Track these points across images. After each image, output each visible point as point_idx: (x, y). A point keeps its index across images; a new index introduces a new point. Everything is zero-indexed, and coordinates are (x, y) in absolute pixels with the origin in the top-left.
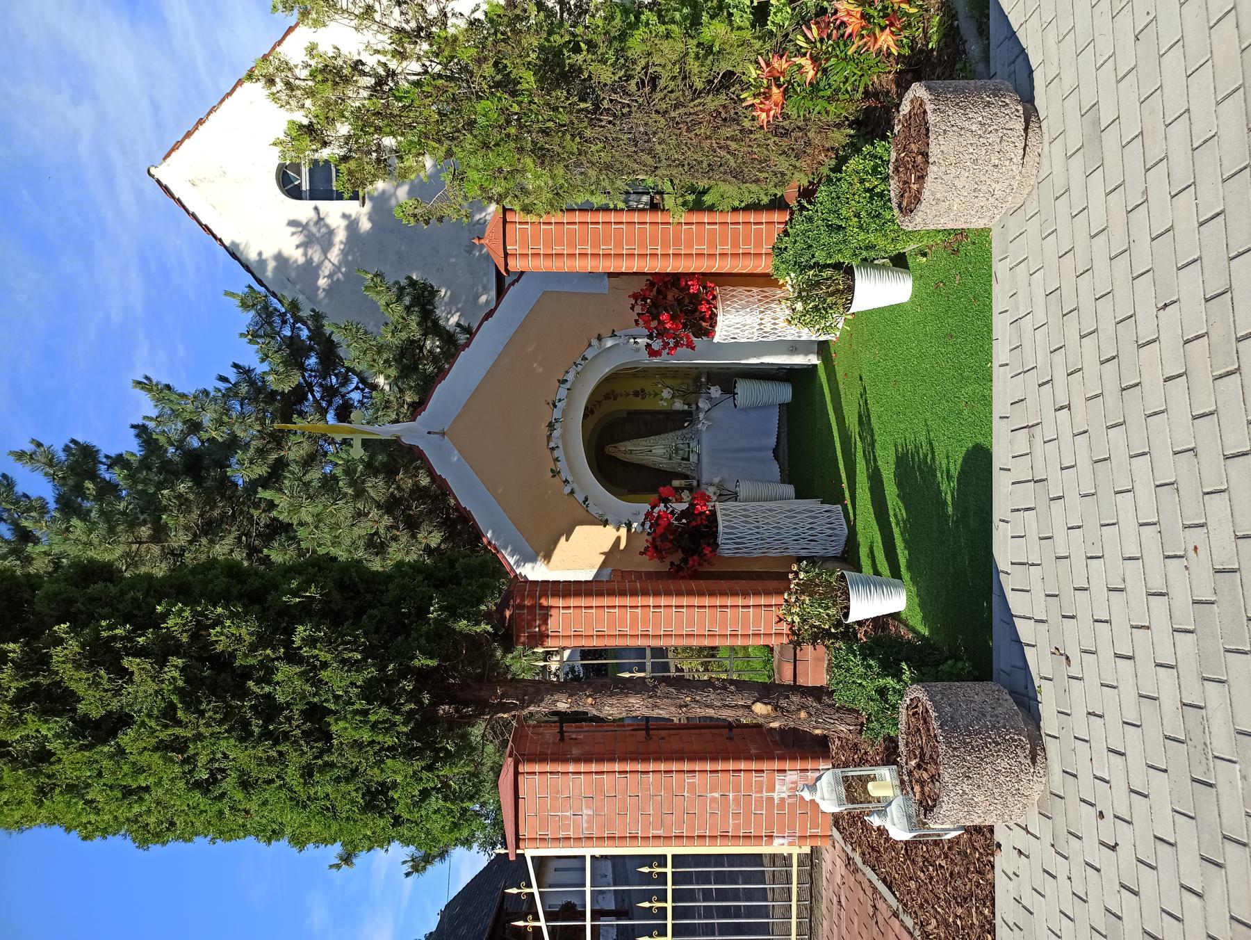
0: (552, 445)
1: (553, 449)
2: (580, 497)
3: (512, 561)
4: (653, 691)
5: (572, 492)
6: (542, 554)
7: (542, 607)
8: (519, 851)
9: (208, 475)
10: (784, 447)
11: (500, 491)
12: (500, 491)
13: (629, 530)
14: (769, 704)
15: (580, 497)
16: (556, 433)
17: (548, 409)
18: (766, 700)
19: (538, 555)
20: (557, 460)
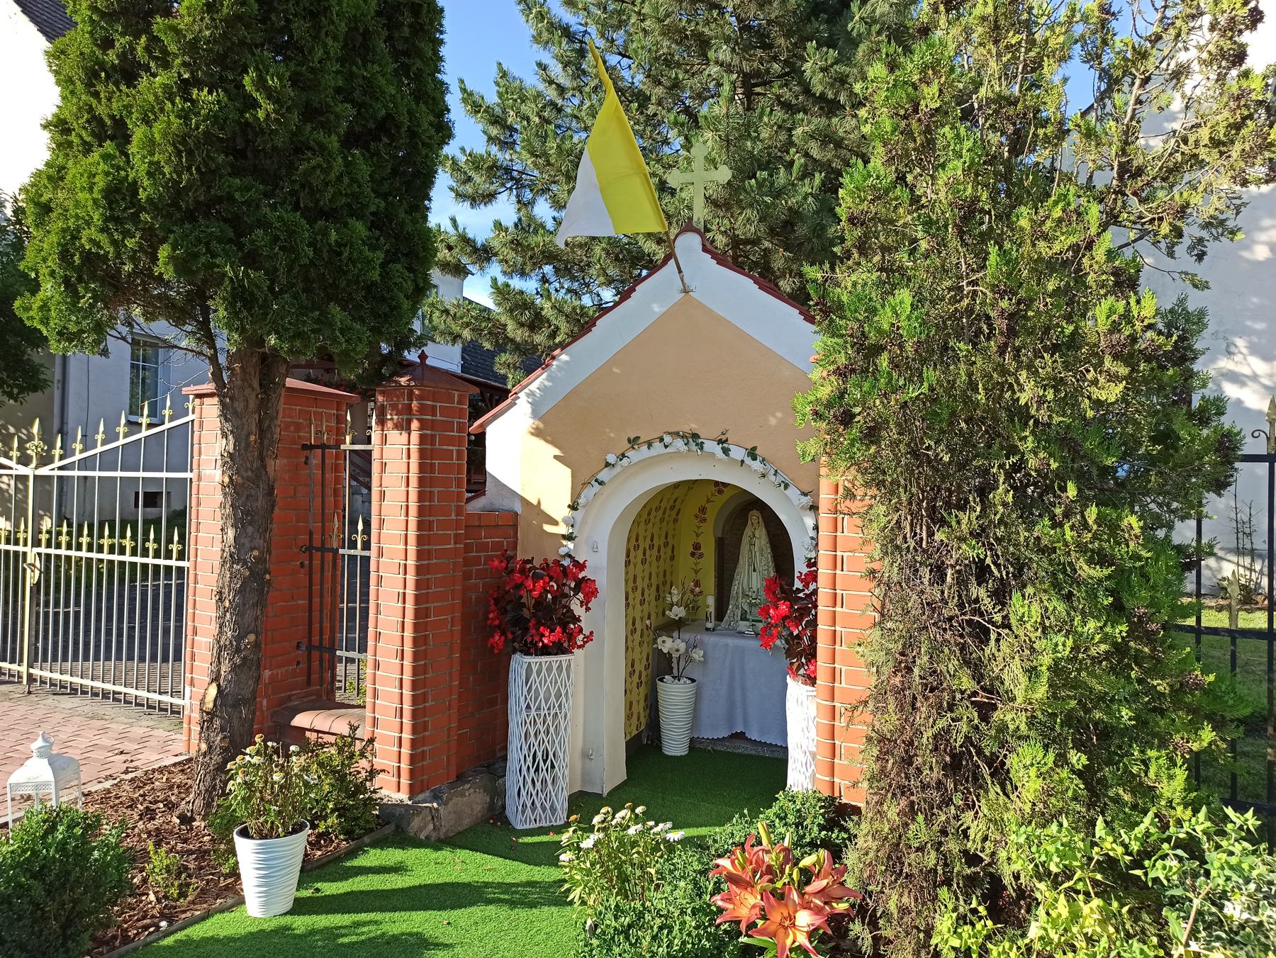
0: (667, 439)
1: (661, 440)
2: (604, 475)
3: (534, 387)
4: (239, 560)
5: (607, 465)
6: (541, 426)
7: (409, 422)
8: (191, 397)
9: (821, 23)
10: (742, 748)
11: (615, 370)
12: (615, 370)
13: (564, 537)
14: (215, 705)
15: (604, 475)
16: (679, 444)
17: (716, 434)
18: (219, 702)
19: (540, 419)
20: (650, 445)
